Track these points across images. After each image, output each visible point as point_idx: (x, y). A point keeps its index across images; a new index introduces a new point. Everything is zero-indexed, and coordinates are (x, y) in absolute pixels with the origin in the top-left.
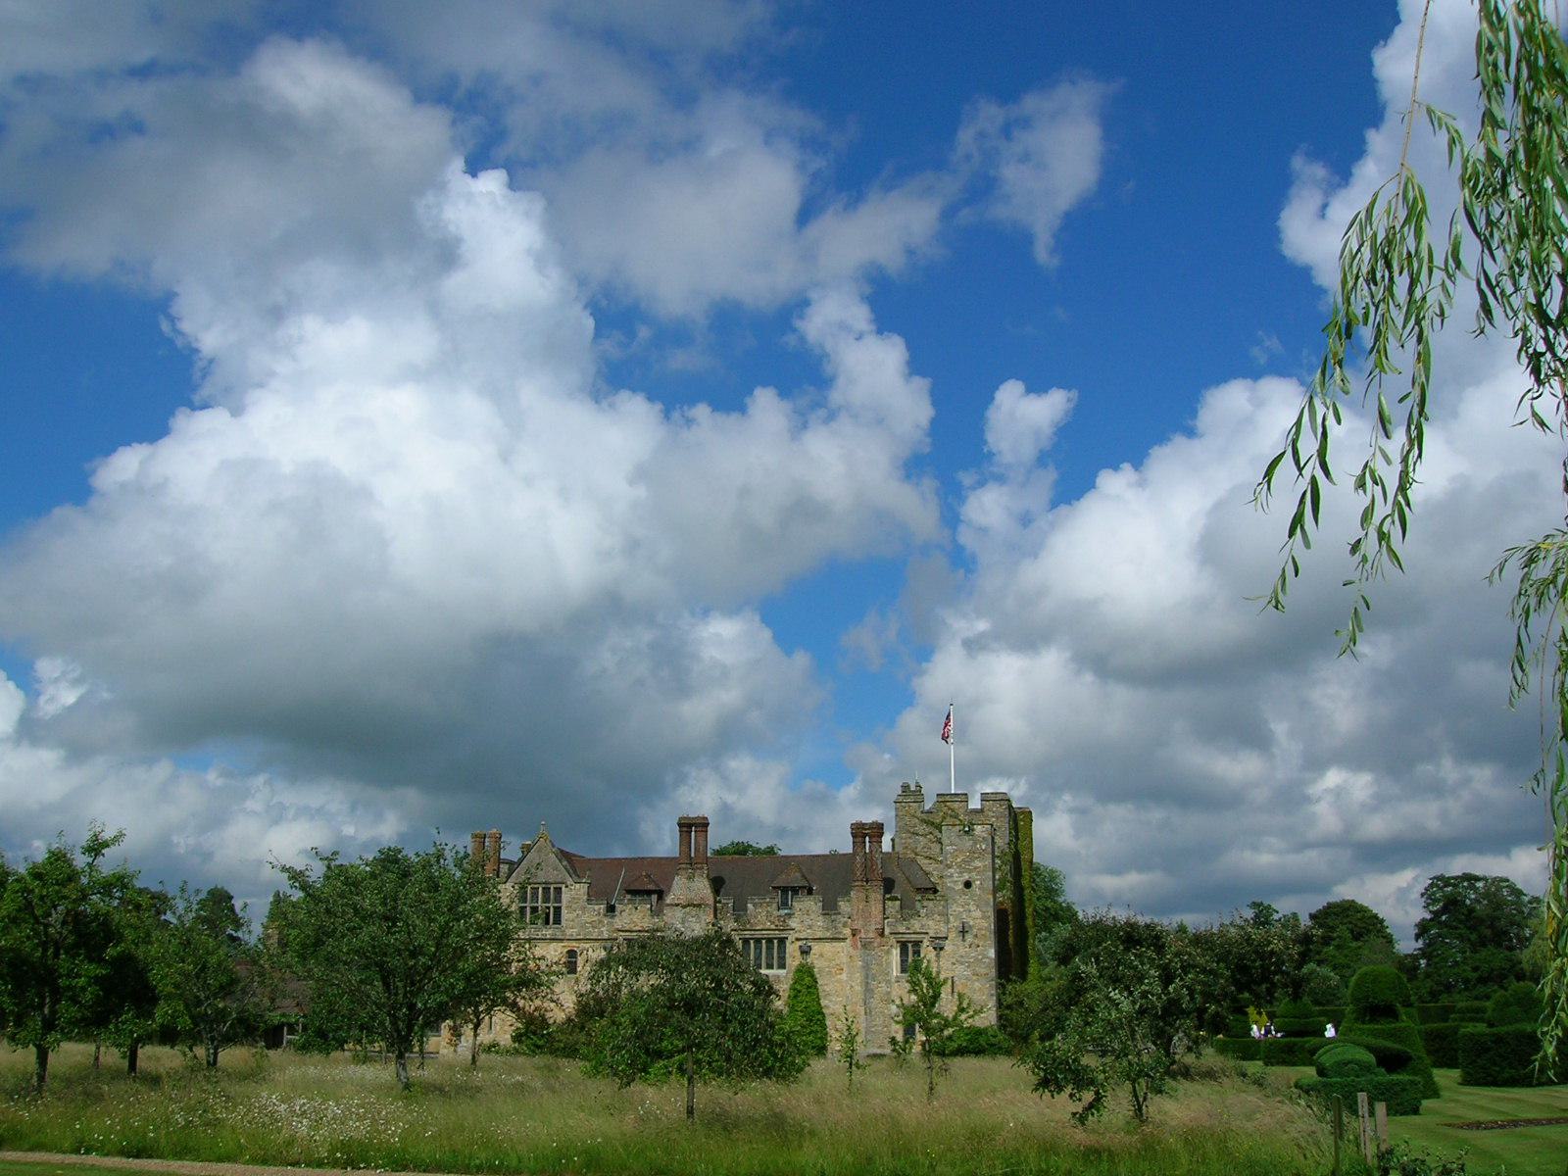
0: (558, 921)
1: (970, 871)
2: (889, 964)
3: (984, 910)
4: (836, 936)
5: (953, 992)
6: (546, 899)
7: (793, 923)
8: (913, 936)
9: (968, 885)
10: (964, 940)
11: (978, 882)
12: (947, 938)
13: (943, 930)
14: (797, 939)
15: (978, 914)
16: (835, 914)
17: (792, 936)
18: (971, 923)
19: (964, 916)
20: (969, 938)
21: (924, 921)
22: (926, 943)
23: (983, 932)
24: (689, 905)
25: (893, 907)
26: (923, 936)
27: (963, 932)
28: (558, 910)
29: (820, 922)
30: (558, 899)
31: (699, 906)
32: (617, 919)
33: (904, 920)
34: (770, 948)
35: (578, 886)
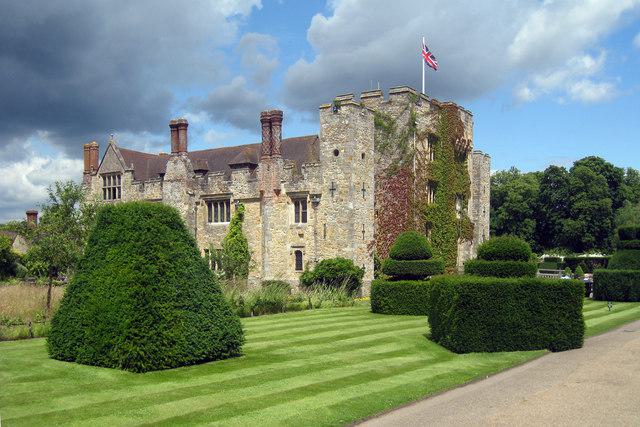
0: (119, 197)
1: (337, 142)
9: (336, 153)
10: (332, 196)
15: (342, 176)
17: (232, 200)
20: (335, 193)
21: (306, 183)
25: (287, 174)
27: (333, 190)
28: (119, 188)
30: (120, 183)
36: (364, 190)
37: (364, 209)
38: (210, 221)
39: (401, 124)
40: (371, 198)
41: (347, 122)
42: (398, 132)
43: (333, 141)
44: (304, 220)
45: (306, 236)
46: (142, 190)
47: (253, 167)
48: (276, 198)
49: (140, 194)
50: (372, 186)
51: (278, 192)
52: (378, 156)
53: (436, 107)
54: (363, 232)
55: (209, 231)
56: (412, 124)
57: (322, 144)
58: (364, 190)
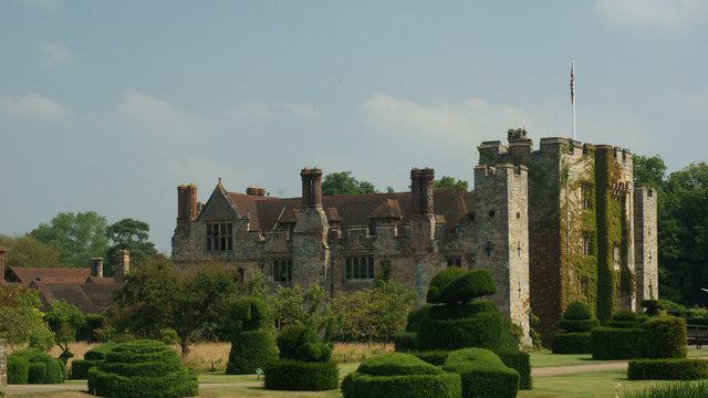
0: (230, 248)
6: (223, 232)
7: (377, 245)
9: (492, 213)
10: (489, 255)
13: (474, 247)
20: (492, 254)
30: (230, 232)
36: (519, 249)
38: (349, 277)
50: (527, 244)
58: (519, 249)
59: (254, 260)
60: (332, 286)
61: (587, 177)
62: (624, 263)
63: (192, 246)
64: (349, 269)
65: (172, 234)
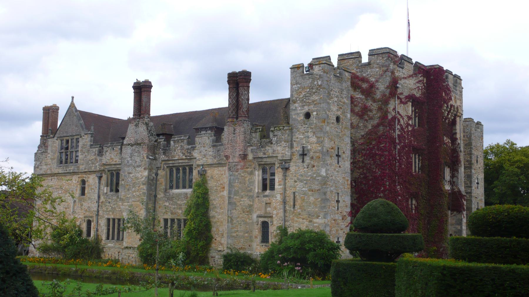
2: (252, 183)
3: (319, 135)
4: (220, 162)
5: (294, 205)
7: (196, 154)
8: (268, 160)
9: (308, 115)
10: (303, 162)
11: (315, 113)
12: (290, 160)
14: (198, 166)
15: (314, 139)
16: (220, 145)
18: (309, 147)
19: (304, 142)
20: (307, 159)
21: (275, 147)
22: (277, 165)
23: (318, 154)
24: (135, 144)
26: (275, 159)
27: (303, 155)
29: (211, 152)
30: (77, 146)
31: (139, 144)
32: (103, 158)
33: (262, 147)
34: (184, 173)
35: (86, 136)
36: (338, 156)
37: (339, 175)
38: (171, 188)
39: (382, 87)
40: (347, 164)
41: (320, 83)
42: (378, 95)
43: (304, 103)
44: (272, 188)
45: (274, 205)
46: (101, 153)
47: (218, 131)
48: (242, 164)
49: (98, 158)
50: (348, 153)
51: (244, 157)
52: (356, 120)
53: (419, 69)
54: (338, 201)
55: (170, 199)
56: (394, 84)
57: (292, 107)
58: (338, 156)
59: (94, 172)
60: (155, 196)
61: (418, 94)
62: (452, 183)
63: (49, 161)
64: (171, 181)
65: (35, 150)
